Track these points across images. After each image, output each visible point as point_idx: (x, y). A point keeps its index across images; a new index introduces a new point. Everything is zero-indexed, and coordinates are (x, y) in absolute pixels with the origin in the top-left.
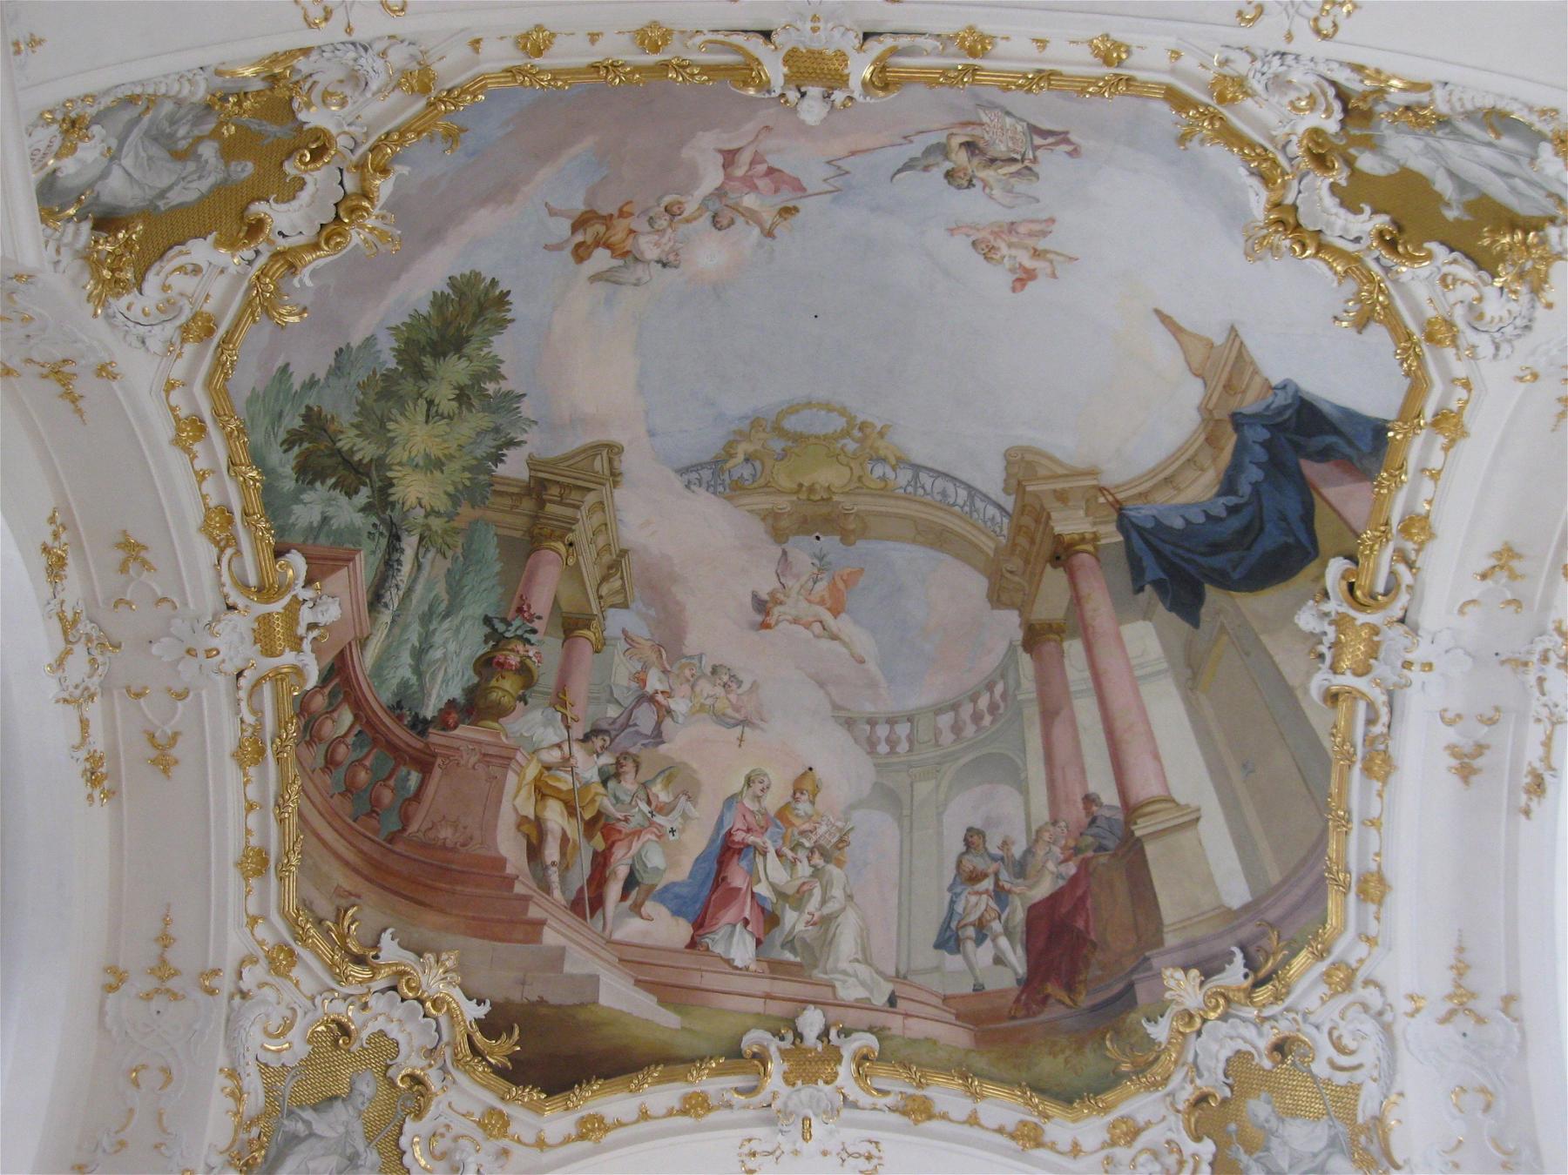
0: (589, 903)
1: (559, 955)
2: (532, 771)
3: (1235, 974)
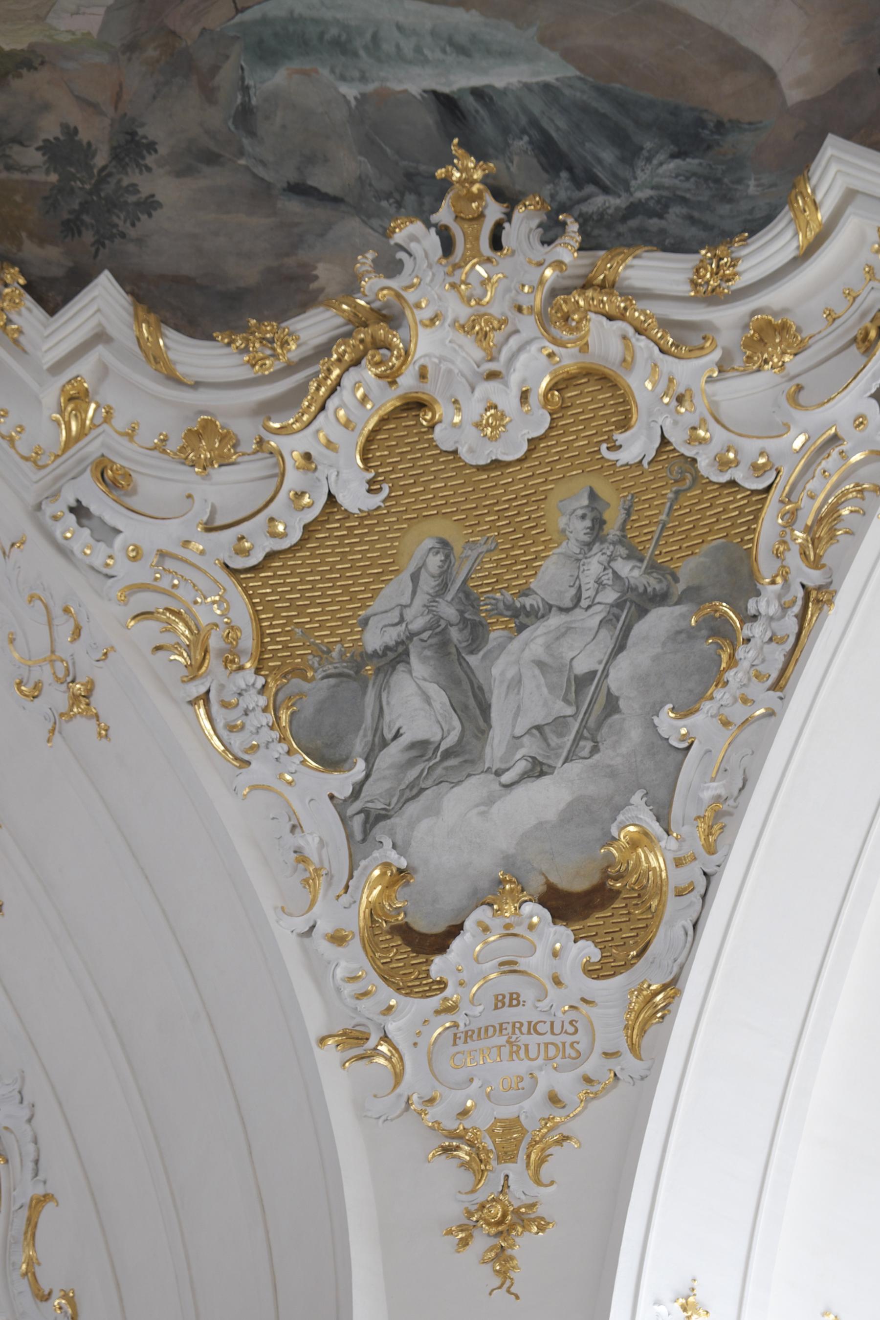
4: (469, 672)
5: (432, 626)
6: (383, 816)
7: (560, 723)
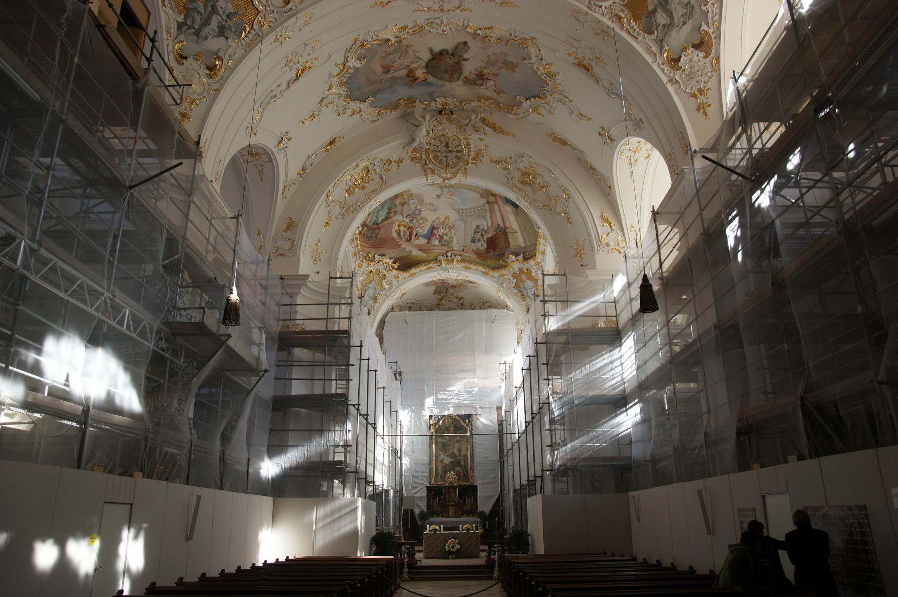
0: (409, 239)
1: (405, 248)
2: (397, 223)
3: (521, 257)
4: (668, 10)
5: (658, 3)
6: (662, 40)
7: (686, 13)
